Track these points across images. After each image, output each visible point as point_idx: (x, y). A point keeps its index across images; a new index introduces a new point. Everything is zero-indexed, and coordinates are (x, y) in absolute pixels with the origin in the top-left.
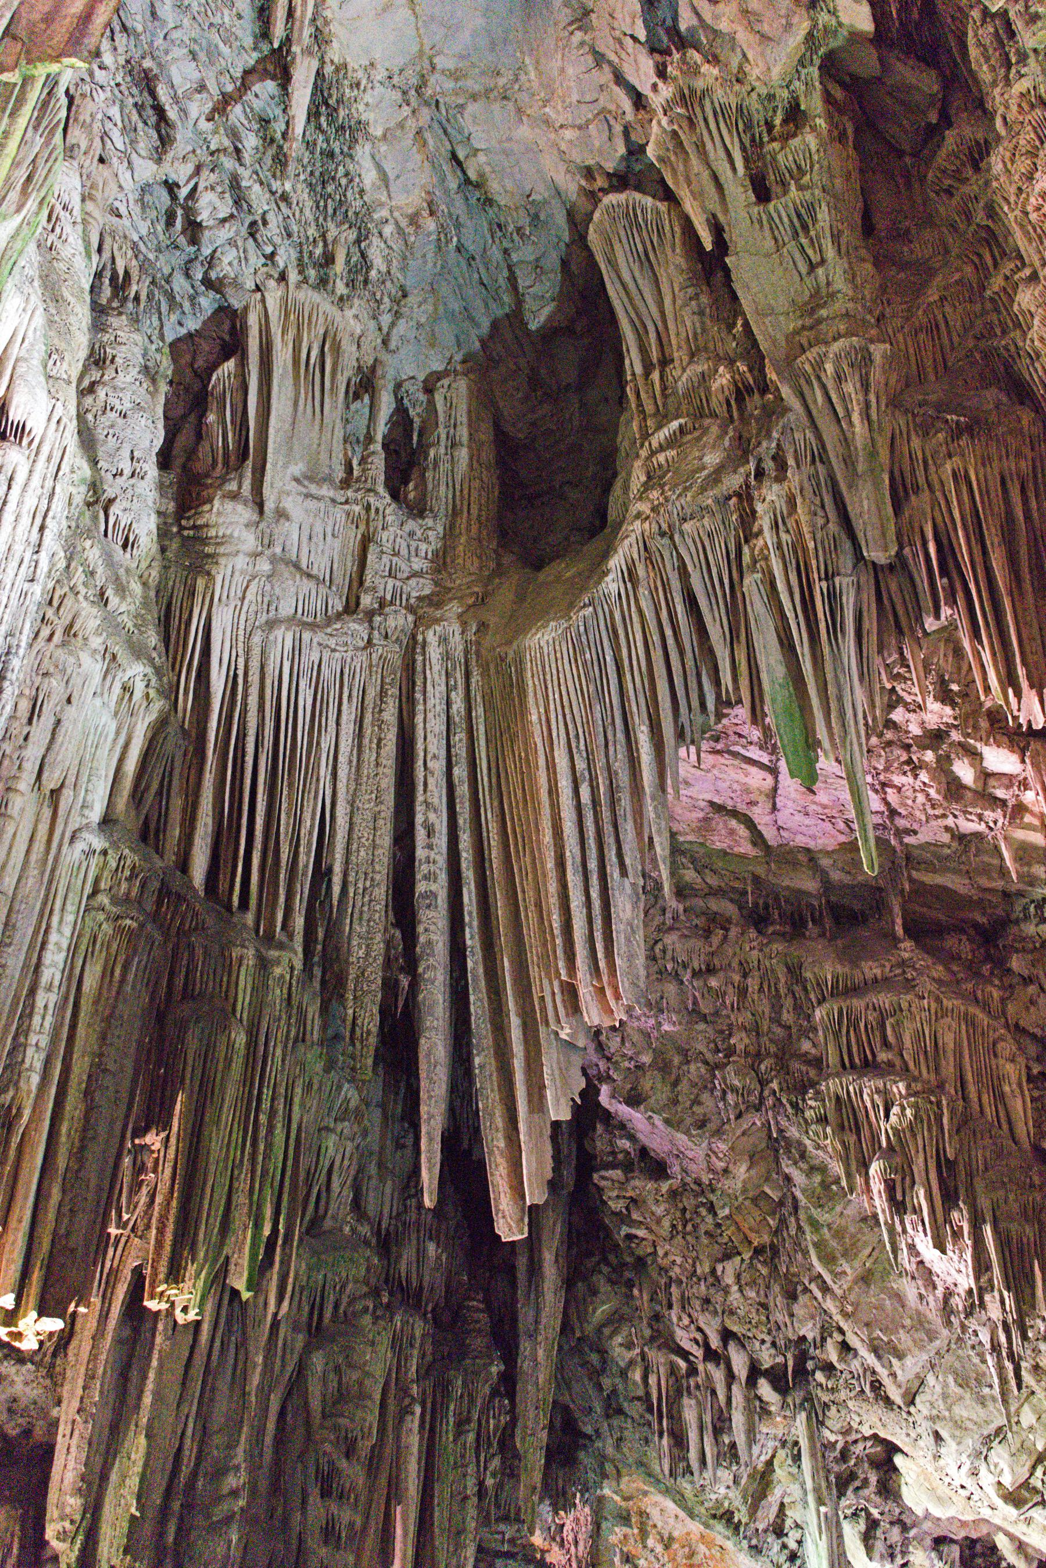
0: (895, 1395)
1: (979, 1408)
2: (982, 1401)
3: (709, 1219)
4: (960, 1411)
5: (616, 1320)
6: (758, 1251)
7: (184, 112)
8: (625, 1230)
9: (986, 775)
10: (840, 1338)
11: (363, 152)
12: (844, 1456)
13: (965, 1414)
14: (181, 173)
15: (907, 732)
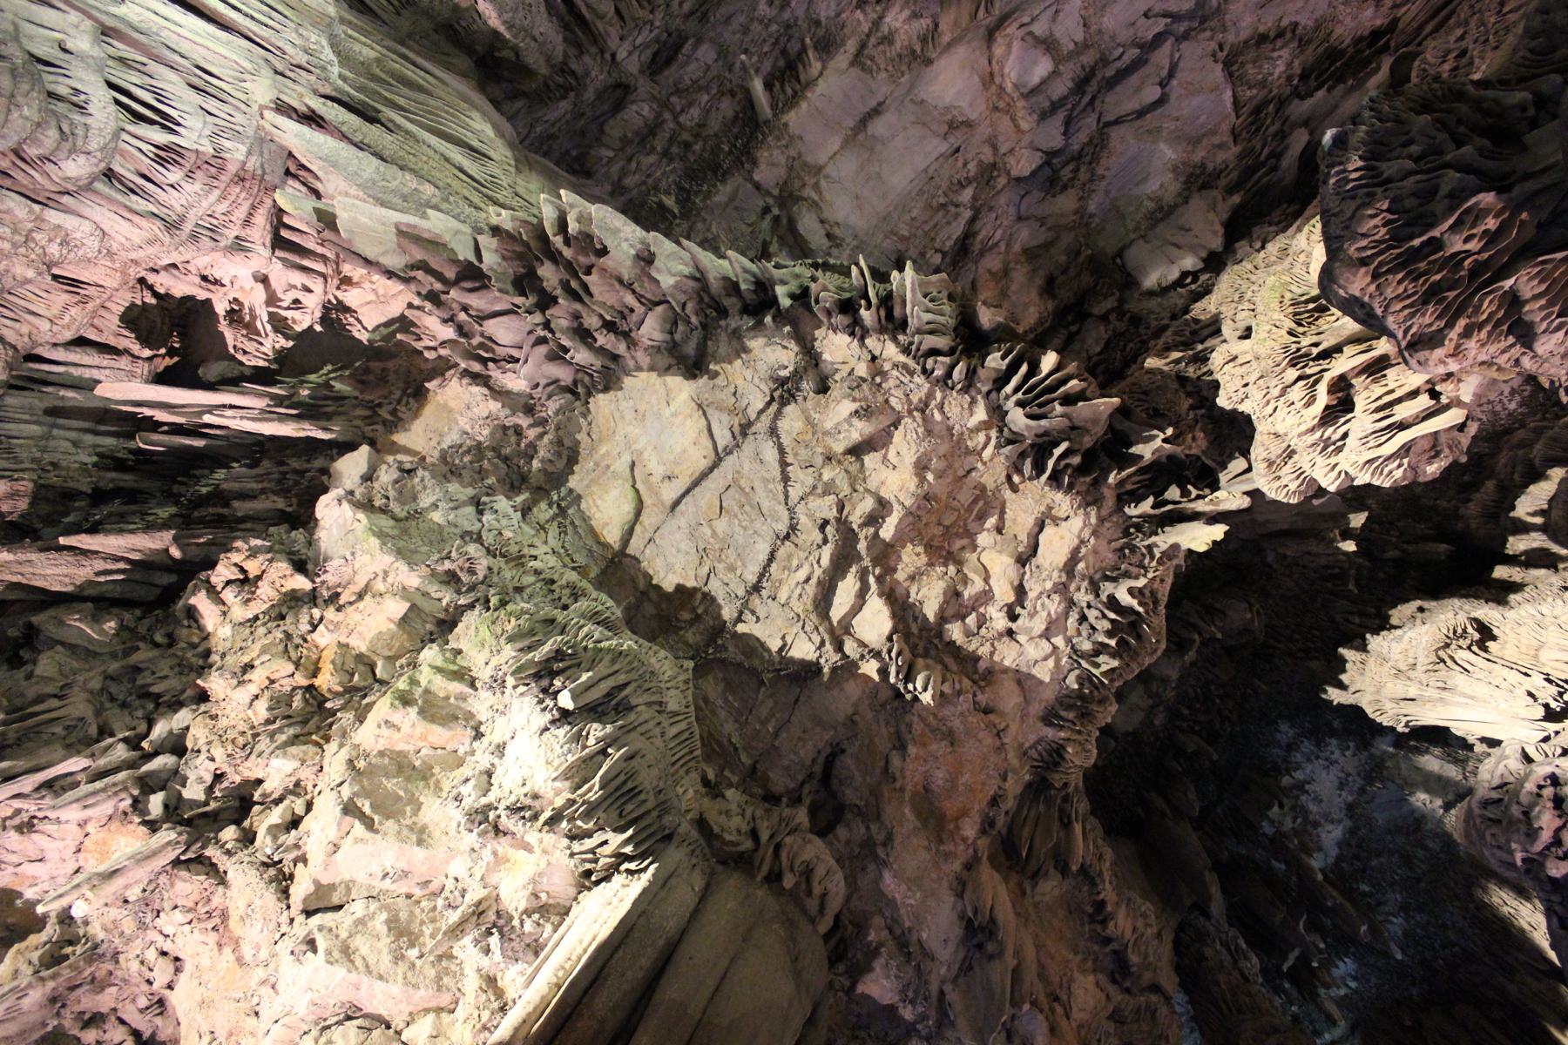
0: (300, 890)
1: (386, 959)
2: (398, 958)
3: (304, 627)
4: (362, 945)
5: (84, 652)
6: (310, 688)
7: (686, 63)
8: (200, 601)
9: (847, 626)
10: (299, 808)
11: (735, 181)
12: (94, 1020)
13: (364, 950)
14: (644, 86)
15: (864, 480)
